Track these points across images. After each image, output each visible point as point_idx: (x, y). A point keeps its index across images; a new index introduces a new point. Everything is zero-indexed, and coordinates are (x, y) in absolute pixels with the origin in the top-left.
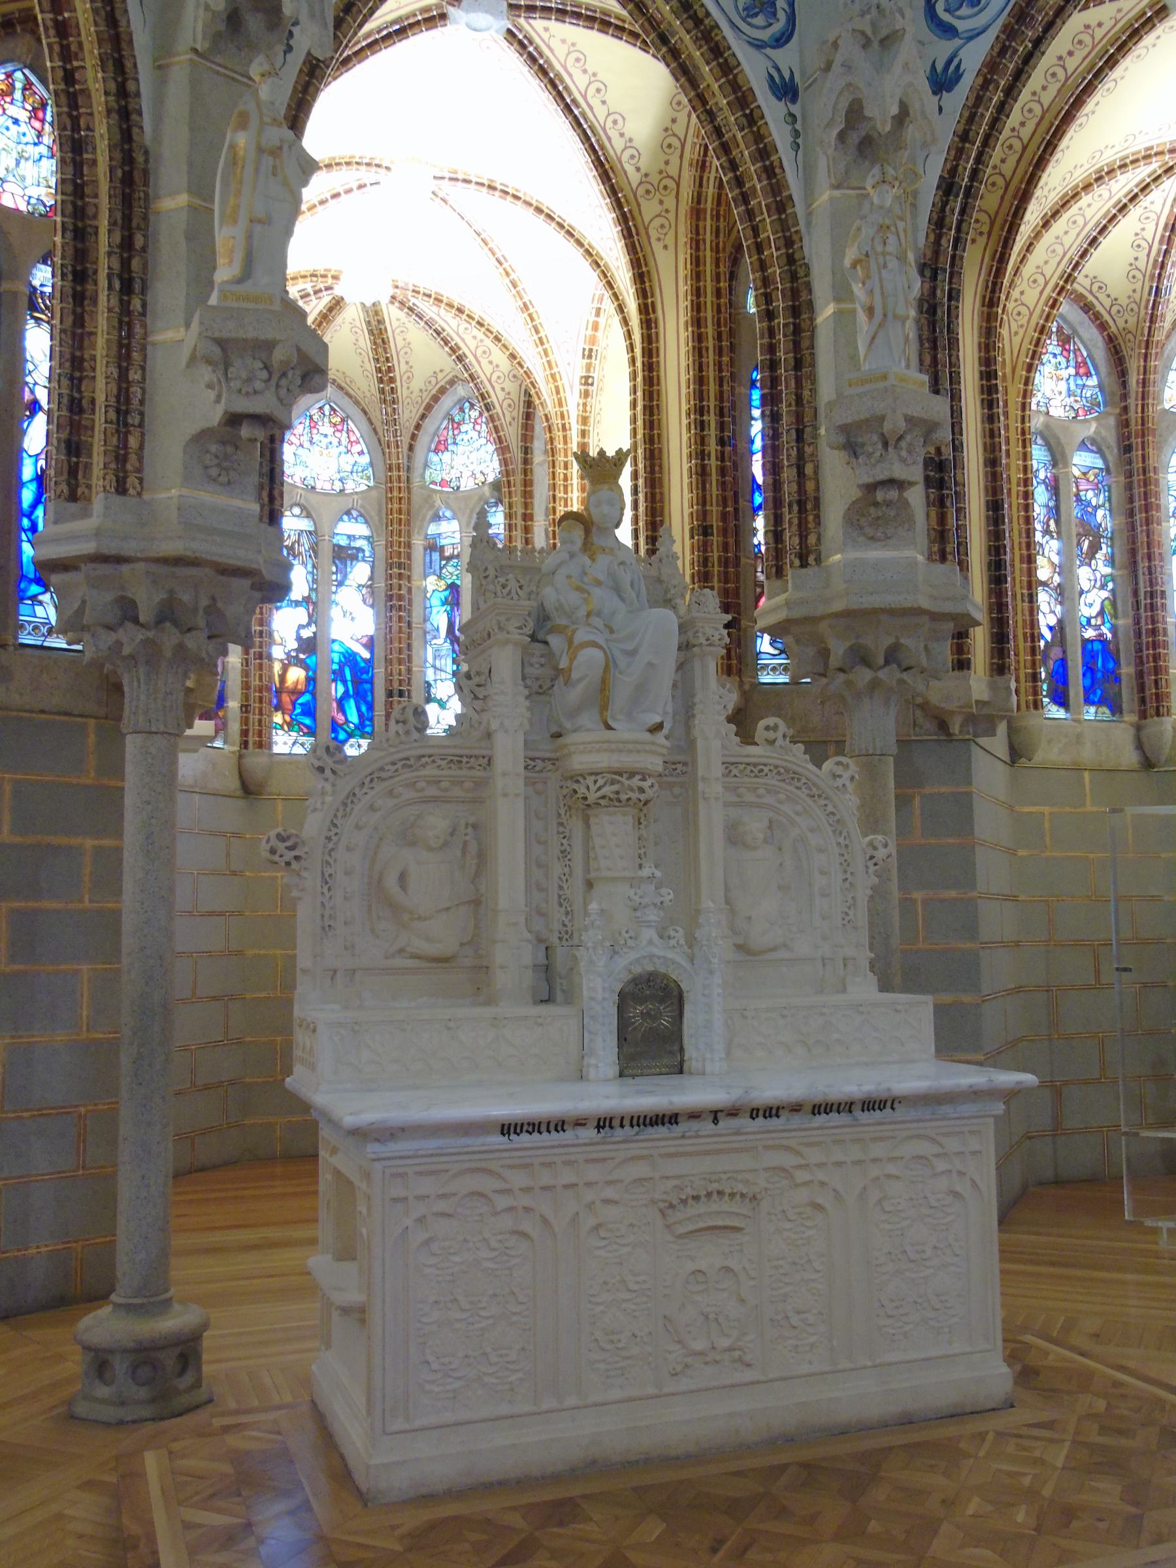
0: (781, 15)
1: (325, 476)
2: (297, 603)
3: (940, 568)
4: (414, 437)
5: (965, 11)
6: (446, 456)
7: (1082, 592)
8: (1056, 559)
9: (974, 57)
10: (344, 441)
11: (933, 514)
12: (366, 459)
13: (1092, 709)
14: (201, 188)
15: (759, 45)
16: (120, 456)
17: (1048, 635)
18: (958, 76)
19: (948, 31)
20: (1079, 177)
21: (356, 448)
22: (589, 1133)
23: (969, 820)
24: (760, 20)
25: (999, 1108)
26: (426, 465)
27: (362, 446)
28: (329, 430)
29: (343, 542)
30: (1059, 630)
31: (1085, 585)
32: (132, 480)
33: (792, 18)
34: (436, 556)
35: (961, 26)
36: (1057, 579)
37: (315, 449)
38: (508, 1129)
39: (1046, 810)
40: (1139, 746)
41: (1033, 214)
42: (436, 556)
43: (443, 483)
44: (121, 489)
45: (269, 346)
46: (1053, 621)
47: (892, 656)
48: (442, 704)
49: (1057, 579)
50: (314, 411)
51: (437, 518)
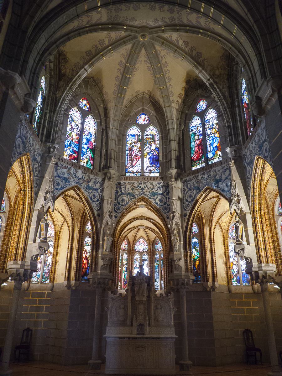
0: (168, 209)
1: (141, 249)
2: (137, 268)
3: (186, 273)
4: (153, 243)
5: (187, 208)
6: (157, 246)
7: (241, 266)
8: (237, 261)
9: (188, 213)
10: (144, 244)
11: (186, 267)
12: (147, 246)
13: (245, 284)
14: (103, 241)
15: (165, 213)
16: (95, 268)
17: (236, 273)
18: (187, 215)
19: (186, 210)
20: (219, 215)
21: (146, 245)
22: (127, 339)
23: (211, 303)
24: (165, 210)
25: (174, 340)
26: (155, 247)
27: (147, 245)
28: (141, 243)
29: (144, 259)
30: (238, 272)
31: (242, 264)
32: (96, 270)
33: (169, 209)
34: (156, 260)
35: (187, 209)
36: (237, 264)
37: (140, 246)
38: (120, 338)
39: (236, 300)
40: (253, 289)
41: (215, 219)
42: (156, 260)
43: (157, 250)
44: (95, 271)
45: (107, 258)
46: (237, 270)
47: (183, 284)
48: (157, 282)
49: (237, 264)
50: (140, 240)
51: (156, 254)
